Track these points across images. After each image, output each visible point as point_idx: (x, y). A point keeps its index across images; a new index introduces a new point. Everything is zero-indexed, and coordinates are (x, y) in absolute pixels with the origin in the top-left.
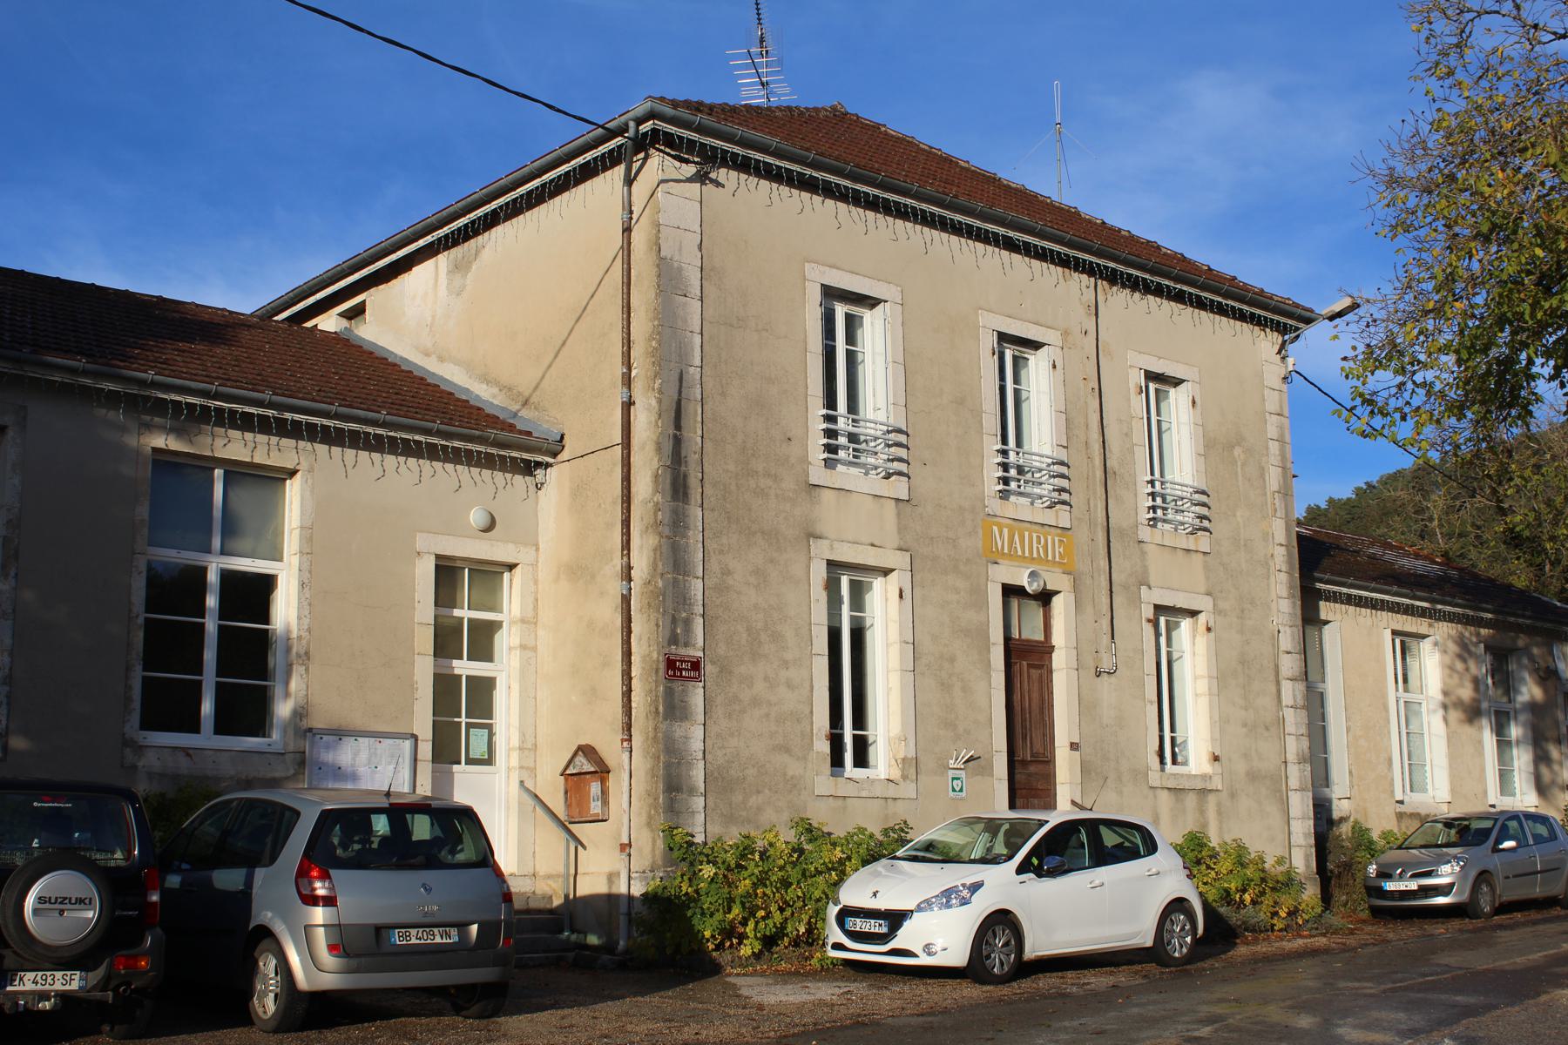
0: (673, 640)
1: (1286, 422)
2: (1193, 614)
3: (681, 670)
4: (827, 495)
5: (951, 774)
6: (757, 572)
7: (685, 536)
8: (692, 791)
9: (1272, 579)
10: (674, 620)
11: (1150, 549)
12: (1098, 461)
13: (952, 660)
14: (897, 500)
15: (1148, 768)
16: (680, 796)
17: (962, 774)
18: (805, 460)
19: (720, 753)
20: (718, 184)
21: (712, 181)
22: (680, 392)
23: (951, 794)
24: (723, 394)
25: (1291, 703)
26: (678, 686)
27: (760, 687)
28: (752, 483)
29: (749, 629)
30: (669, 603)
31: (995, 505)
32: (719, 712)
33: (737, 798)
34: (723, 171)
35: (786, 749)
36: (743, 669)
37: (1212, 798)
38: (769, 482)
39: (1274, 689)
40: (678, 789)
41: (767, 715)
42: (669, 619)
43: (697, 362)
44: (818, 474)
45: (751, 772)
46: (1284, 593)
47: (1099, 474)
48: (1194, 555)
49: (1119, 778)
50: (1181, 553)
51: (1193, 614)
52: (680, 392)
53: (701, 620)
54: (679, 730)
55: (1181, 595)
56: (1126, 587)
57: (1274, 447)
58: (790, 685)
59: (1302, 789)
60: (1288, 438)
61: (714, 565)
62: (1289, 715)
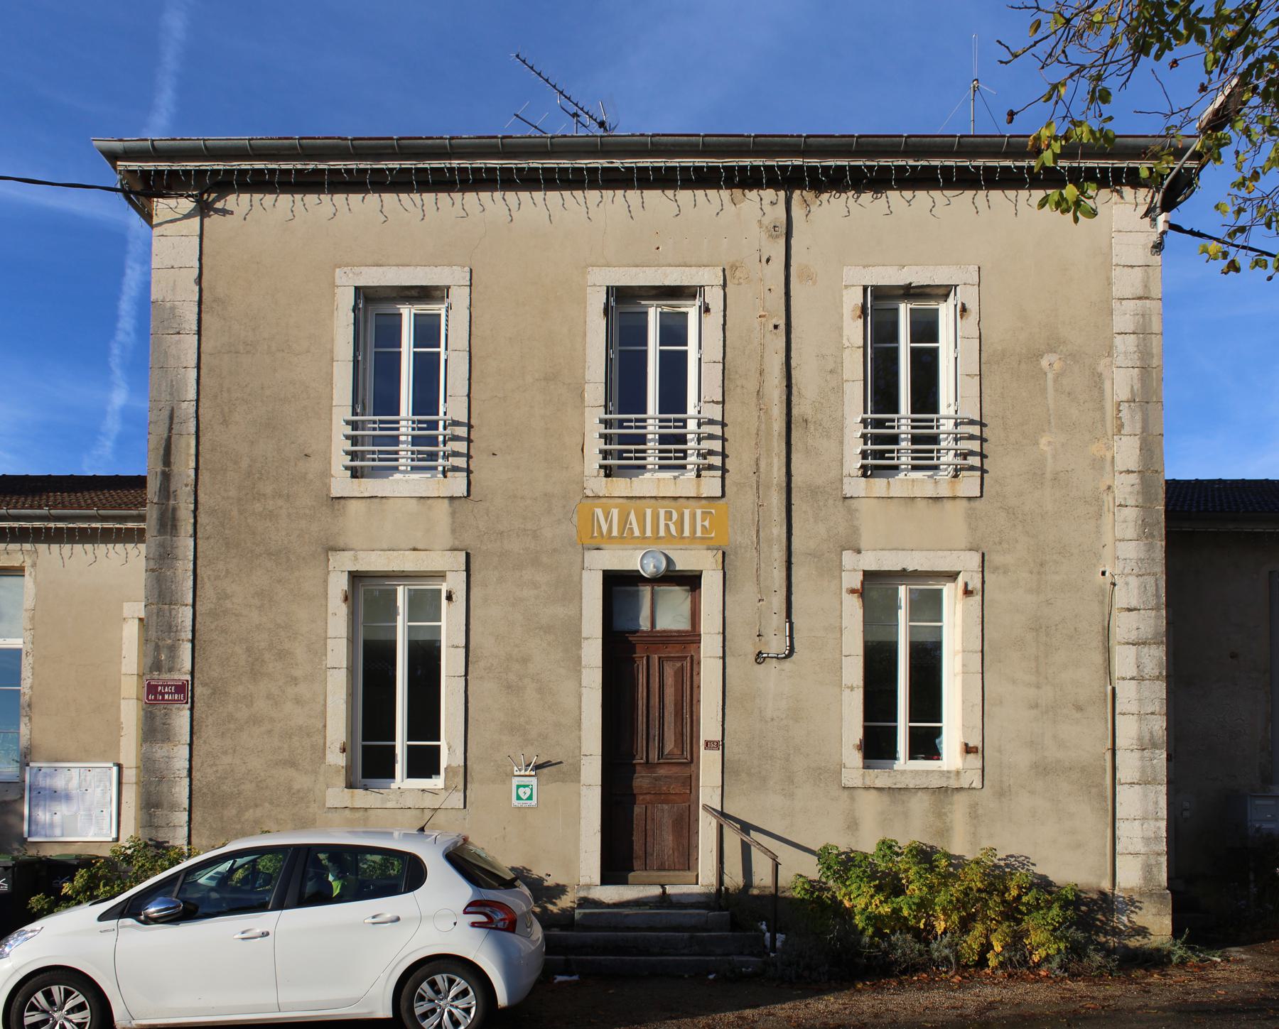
0: (157, 666)
1: (1155, 306)
2: (952, 576)
3: (163, 694)
4: (353, 505)
5: (515, 781)
6: (260, 594)
7: (171, 567)
8: (173, 807)
9: (1107, 519)
10: (157, 648)
11: (863, 506)
12: (778, 412)
13: (525, 660)
14: (452, 498)
15: (842, 765)
16: (159, 812)
17: (534, 781)
18: (326, 474)
19: (209, 771)
20: (224, 212)
21: (217, 211)
22: (170, 429)
23: (515, 802)
24: (225, 422)
25: (1133, 672)
26: (159, 711)
27: (261, 706)
28: (258, 507)
29: (249, 650)
30: (153, 634)
31: (599, 485)
32: (208, 732)
33: (231, 812)
34: (232, 198)
35: (293, 764)
36: (240, 689)
37: (960, 801)
38: (280, 502)
39: (1098, 658)
40: (158, 805)
41: (270, 732)
42: (151, 646)
43: (192, 395)
44: (341, 484)
45: (248, 787)
46: (1131, 532)
47: (778, 425)
48: (949, 505)
49: (790, 780)
50: (921, 504)
51: (952, 576)
52: (170, 429)
53: (189, 645)
54: (160, 751)
55: (916, 554)
56: (815, 555)
57: (1126, 346)
58: (298, 701)
59: (1144, 782)
60: (1156, 326)
61: (207, 590)
62: (1127, 692)
